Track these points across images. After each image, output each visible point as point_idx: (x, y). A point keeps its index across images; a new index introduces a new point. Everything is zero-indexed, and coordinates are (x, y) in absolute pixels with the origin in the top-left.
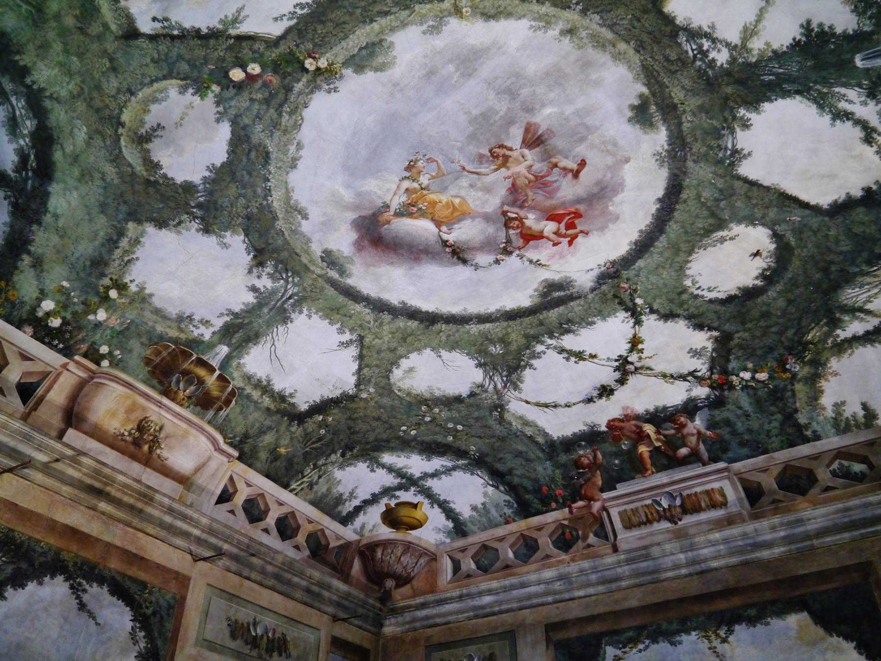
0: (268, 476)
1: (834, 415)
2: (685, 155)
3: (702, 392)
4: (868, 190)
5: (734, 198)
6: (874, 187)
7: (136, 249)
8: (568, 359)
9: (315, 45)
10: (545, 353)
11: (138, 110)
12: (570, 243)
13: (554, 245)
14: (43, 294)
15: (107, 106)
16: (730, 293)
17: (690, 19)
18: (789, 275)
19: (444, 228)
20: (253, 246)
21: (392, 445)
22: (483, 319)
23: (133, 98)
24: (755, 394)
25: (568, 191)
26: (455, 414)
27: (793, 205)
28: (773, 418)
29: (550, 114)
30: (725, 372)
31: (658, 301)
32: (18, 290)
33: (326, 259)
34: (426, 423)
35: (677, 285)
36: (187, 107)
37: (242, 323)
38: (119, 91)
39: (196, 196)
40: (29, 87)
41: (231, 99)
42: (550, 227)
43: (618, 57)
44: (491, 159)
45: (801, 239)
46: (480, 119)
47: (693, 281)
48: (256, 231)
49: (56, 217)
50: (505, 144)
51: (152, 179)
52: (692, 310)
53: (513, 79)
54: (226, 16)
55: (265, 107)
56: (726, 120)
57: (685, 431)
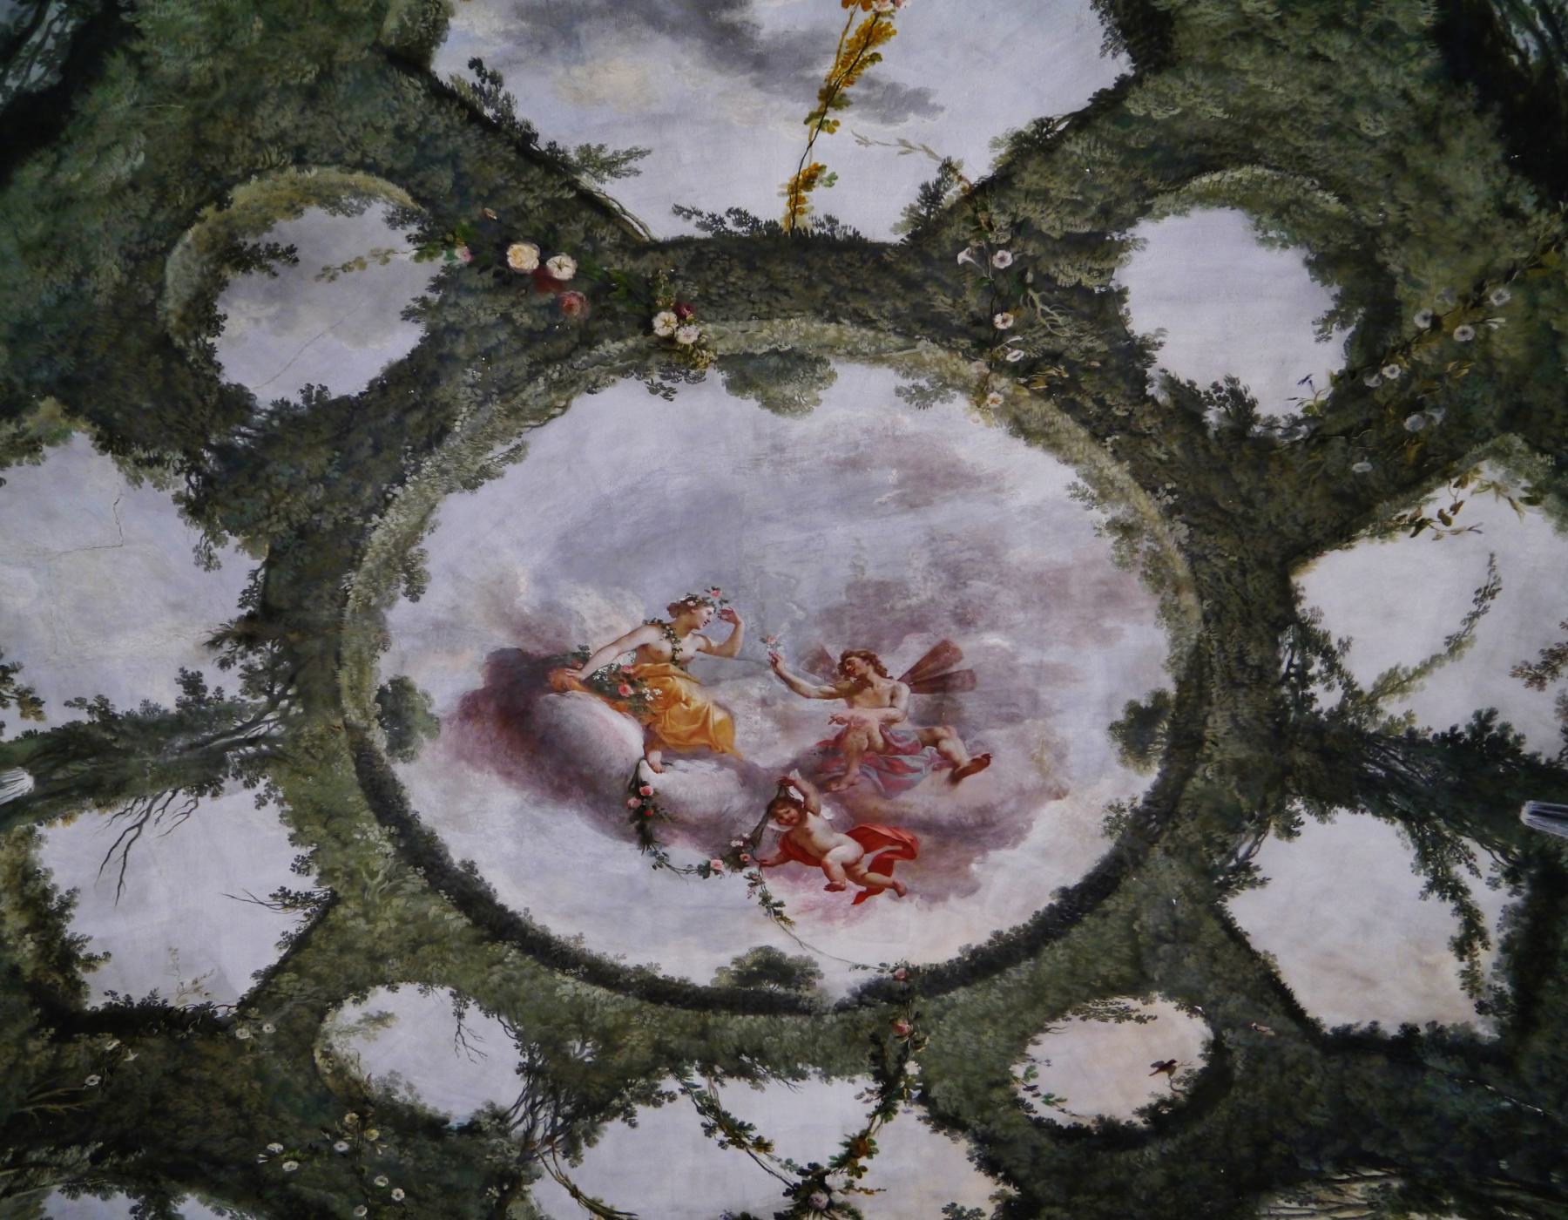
2: (1161, 832)
4: (1409, 1031)
5: (1190, 948)
6: (1423, 1031)
7: (14, 462)
8: (709, 1131)
9: (705, 297)
10: (672, 1097)
11: (281, 198)
12: (860, 898)
13: (828, 888)
15: (229, 150)
16: (1080, 1121)
17: (1322, 614)
18: (1198, 1130)
20: (264, 595)
21: (222, 1177)
22: (600, 973)
23: (292, 170)
25: (926, 796)
26: (408, 1160)
27: (1277, 1005)
29: (993, 647)
31: (946, 1082)
33: (389, 701)
34: (333, 1154)
35: (997, 1067)
36: (375, 254)
37: (108, 743)
38: (280, 137)
39: (234, 428)
41: (471, 291)
42: (844, 849)
43: (1169, 612)
44: (836, 671)
45: (1254, 1072)
46: (870, 591)
47: (1029, 1070)
48: (296, 568)
50: (880, 658)
51: (179, 341)
52: (996, 1126)
53: (977, 554)
54: (601, 148)
55: (517, 345)
56: (1264, 805)
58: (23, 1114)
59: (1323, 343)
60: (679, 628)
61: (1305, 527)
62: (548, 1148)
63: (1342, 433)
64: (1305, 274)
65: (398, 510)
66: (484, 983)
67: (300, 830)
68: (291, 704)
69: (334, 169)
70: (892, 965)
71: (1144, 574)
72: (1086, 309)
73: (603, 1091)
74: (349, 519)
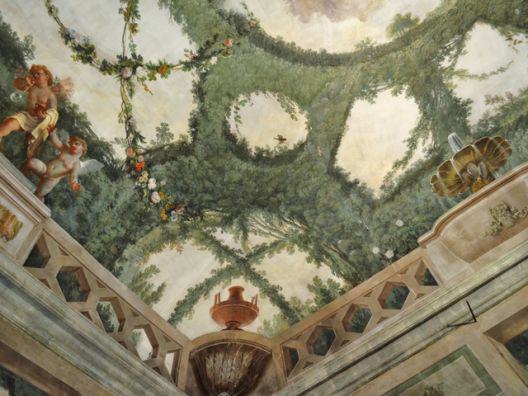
1: (143, 272)
3: (120, 153)
4: (356, 182)
24: (136, 201)
27: (332, 146)
28: (119, 228)
30: (149, 165)
31: (217, 78)
47: (245, 101)
52: (212, 111)
57: (66, 157)
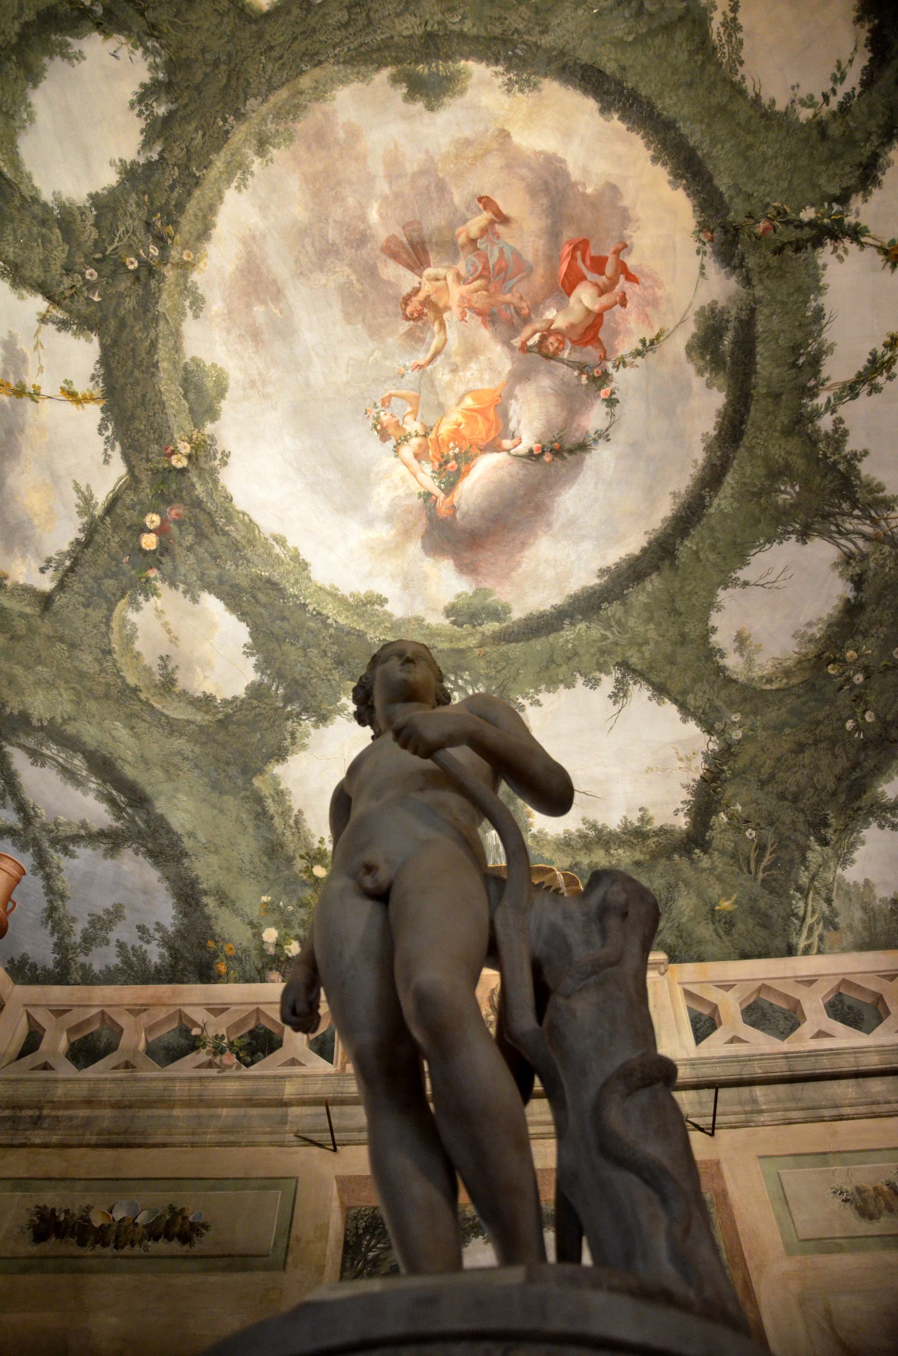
0: (745, 956)
2: (524, 43)
8: (875, 389)
10: (840, 421)
12: (631, 278)
14: (256, 928)
15: (107, 684)
19: (507, 443)
21: (869, 764)
22: (712, 477)
23: (115, 656)
29: (380, 215)
31: (822, 181)
32: (230, 941)
33: (460, 619)
34: (864, 686)
38: (97, 660)
40: (42, 728)
41: (175, 568)
42: (585, 297)
43: (320, 93)
44: (420, 323)
49: (192, 835)
50: (404, 293)
51: (220, 716)
54: (77, 506)
55: (207, 542)
58: (763, 880)
59: (85, 54)
60: (399, 434)
61: (221, 15)
62: (883, 523)
63: (143, 15)
64: (43, 84)
65: (323, 608)
66: (715, 565)
67: (562, 681)
68: (462, 678)
69: (111, 637)
70: (698, 244)
71: (294, 120)
72: (110, 215)
73: (830, 477)
74: (331, 636)
